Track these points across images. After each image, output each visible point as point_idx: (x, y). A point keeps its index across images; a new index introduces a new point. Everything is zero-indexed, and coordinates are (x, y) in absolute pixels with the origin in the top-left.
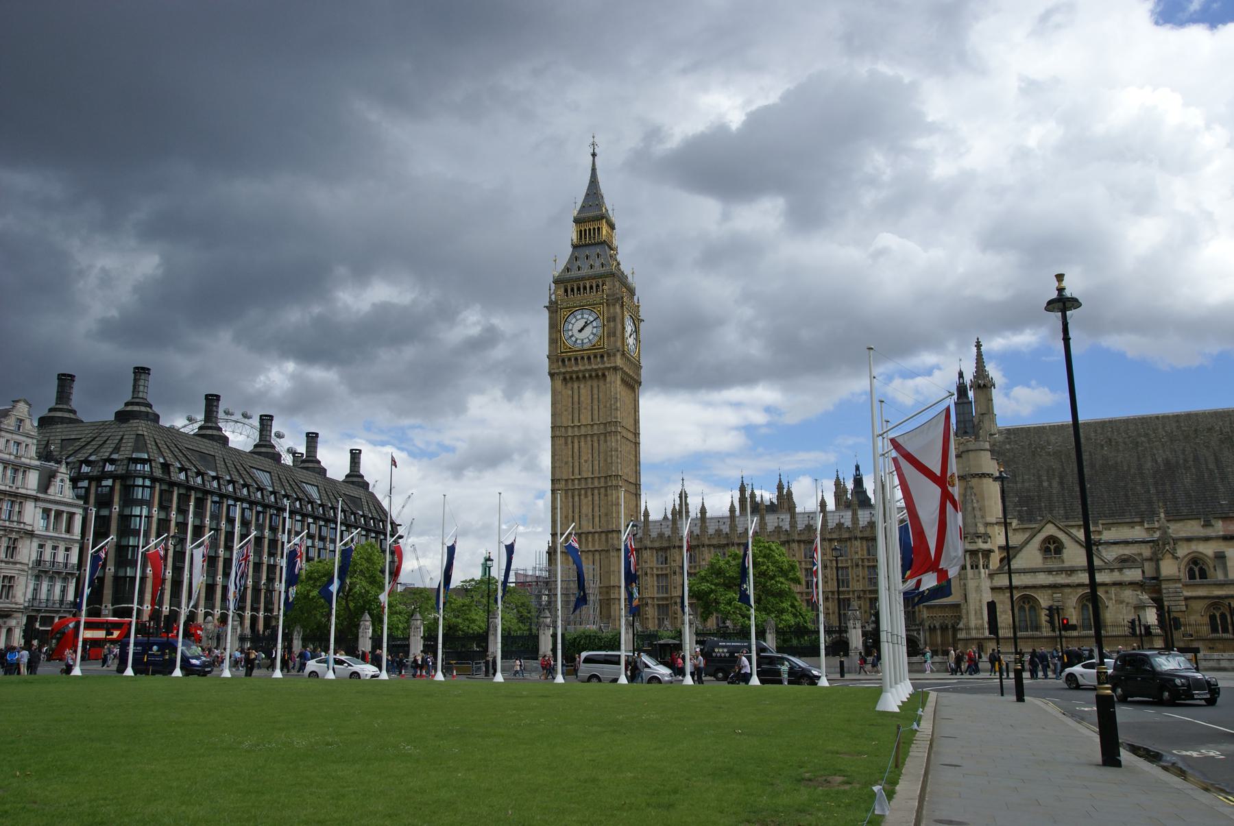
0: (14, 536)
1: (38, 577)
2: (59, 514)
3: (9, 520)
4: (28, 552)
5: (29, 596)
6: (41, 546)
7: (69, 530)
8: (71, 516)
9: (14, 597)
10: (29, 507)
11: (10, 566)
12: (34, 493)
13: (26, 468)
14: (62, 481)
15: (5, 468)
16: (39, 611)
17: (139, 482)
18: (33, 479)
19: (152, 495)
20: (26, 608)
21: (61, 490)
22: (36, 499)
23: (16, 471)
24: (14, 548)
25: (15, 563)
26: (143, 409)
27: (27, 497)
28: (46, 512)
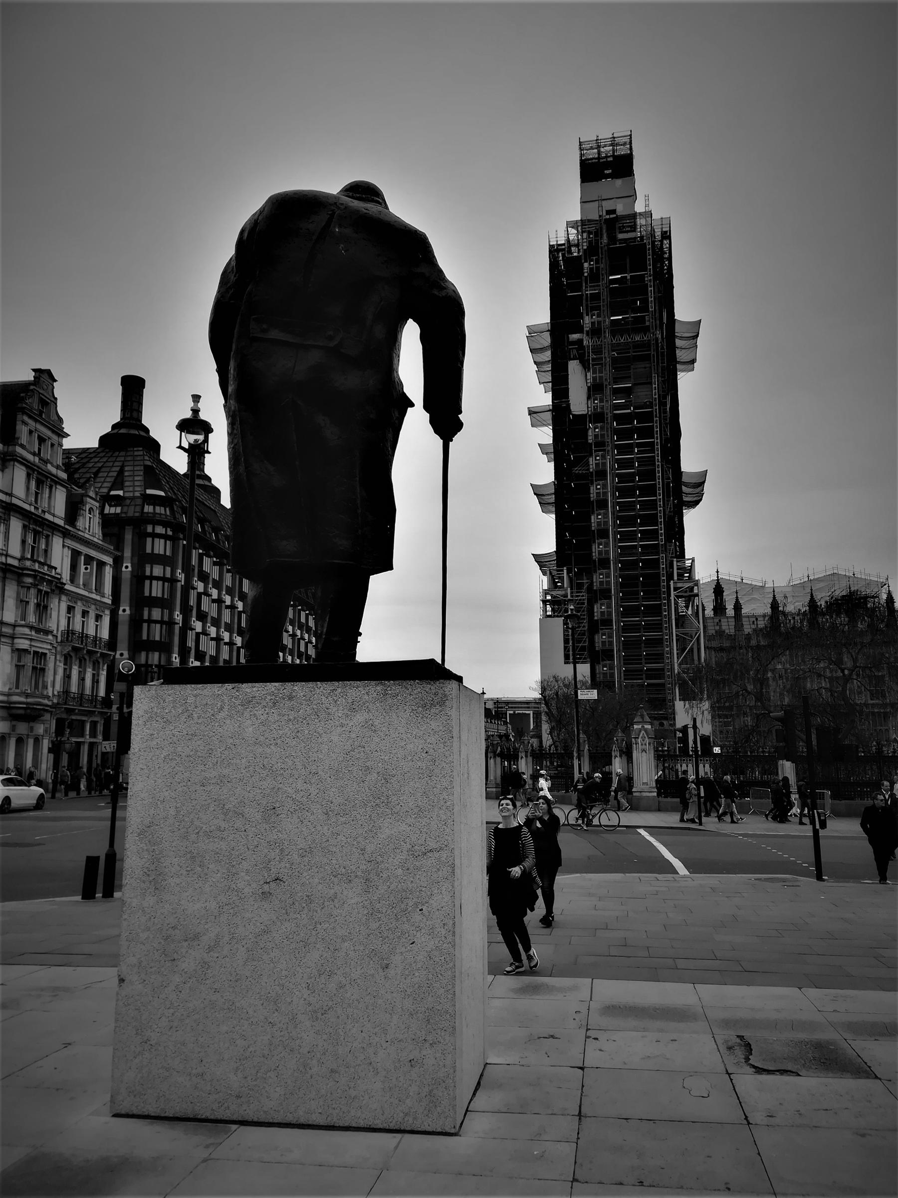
0: (45, 588)
1: (67, 659)
2: (89, 559)
3: (32, 559)
4: (58, 618)
5: (58, 687)
6: (70, 609)
7: (99, 589)
8: (101, 564)
9: (45, 687)
10: (57, 542)
11: (41, 636)
12: (61, 523)
13: (57, 481)
14: (91, 510)
15: (28, 476)
16: (70, 711)
17: (160, 530)
18: (60, 499)
19: (174, 549)
20: (54, 706)
21: (90, 524)
22: (65, 534)
23: (39, 483)
24: (46, 607)
25: (47, 632)
26: (142, 433)
27: (54, 527)
28: (75, 554)
